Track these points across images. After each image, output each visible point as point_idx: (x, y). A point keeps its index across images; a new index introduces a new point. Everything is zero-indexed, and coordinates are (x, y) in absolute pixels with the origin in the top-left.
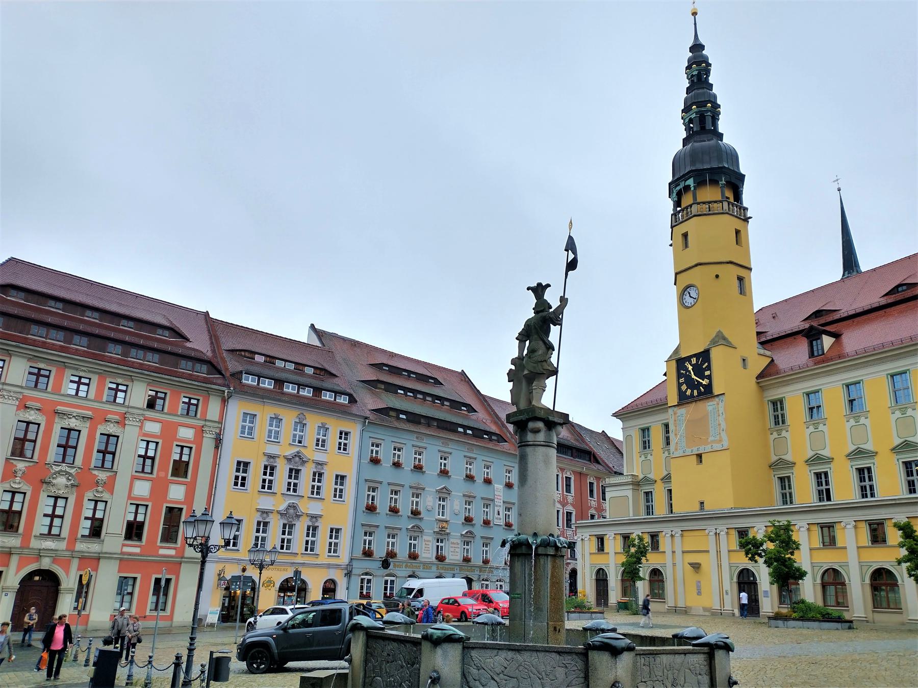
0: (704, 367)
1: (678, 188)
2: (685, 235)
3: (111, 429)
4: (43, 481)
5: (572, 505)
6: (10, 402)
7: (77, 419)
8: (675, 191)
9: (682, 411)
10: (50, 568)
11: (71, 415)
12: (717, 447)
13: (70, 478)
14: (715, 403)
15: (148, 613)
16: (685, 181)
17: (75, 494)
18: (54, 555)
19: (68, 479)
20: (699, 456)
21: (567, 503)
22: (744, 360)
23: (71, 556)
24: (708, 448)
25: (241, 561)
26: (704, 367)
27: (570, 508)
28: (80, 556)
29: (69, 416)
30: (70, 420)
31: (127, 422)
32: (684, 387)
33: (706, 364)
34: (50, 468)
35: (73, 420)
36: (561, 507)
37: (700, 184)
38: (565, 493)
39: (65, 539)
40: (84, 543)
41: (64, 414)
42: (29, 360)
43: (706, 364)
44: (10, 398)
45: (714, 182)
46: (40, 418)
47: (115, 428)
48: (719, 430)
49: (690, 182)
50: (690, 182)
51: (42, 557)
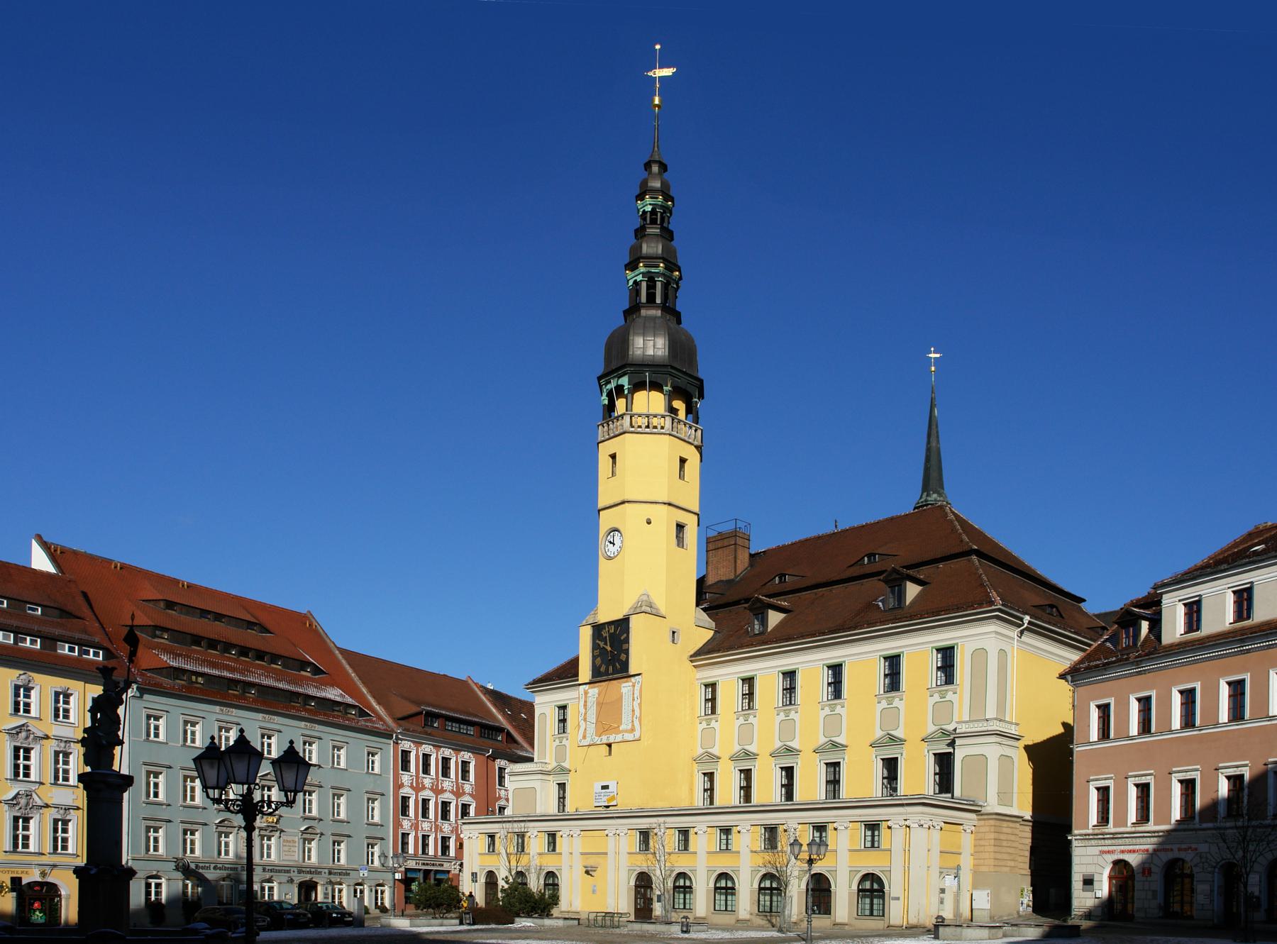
0: (622, 638)
1: (609, 387)
2: (613, 457)
5: (471, 795)
8: (605, 390)
9: (594, 691)
12: (629, 737)
14: (630, 684)
16: (619, 378)
20: (609, 745)
21: (464, 793)
22: (674, 633)
24: (619, 738)
26: (622, 638)
27: (466, 799)
32: (598, 661)
33: (625, 635)
36: (454, 797)
37: (638, 386)
38: (460, 781)
43: (625, 635)
45: (656, 386)
48: (633, 717)
49: (624, 381)
50: (624, 381)
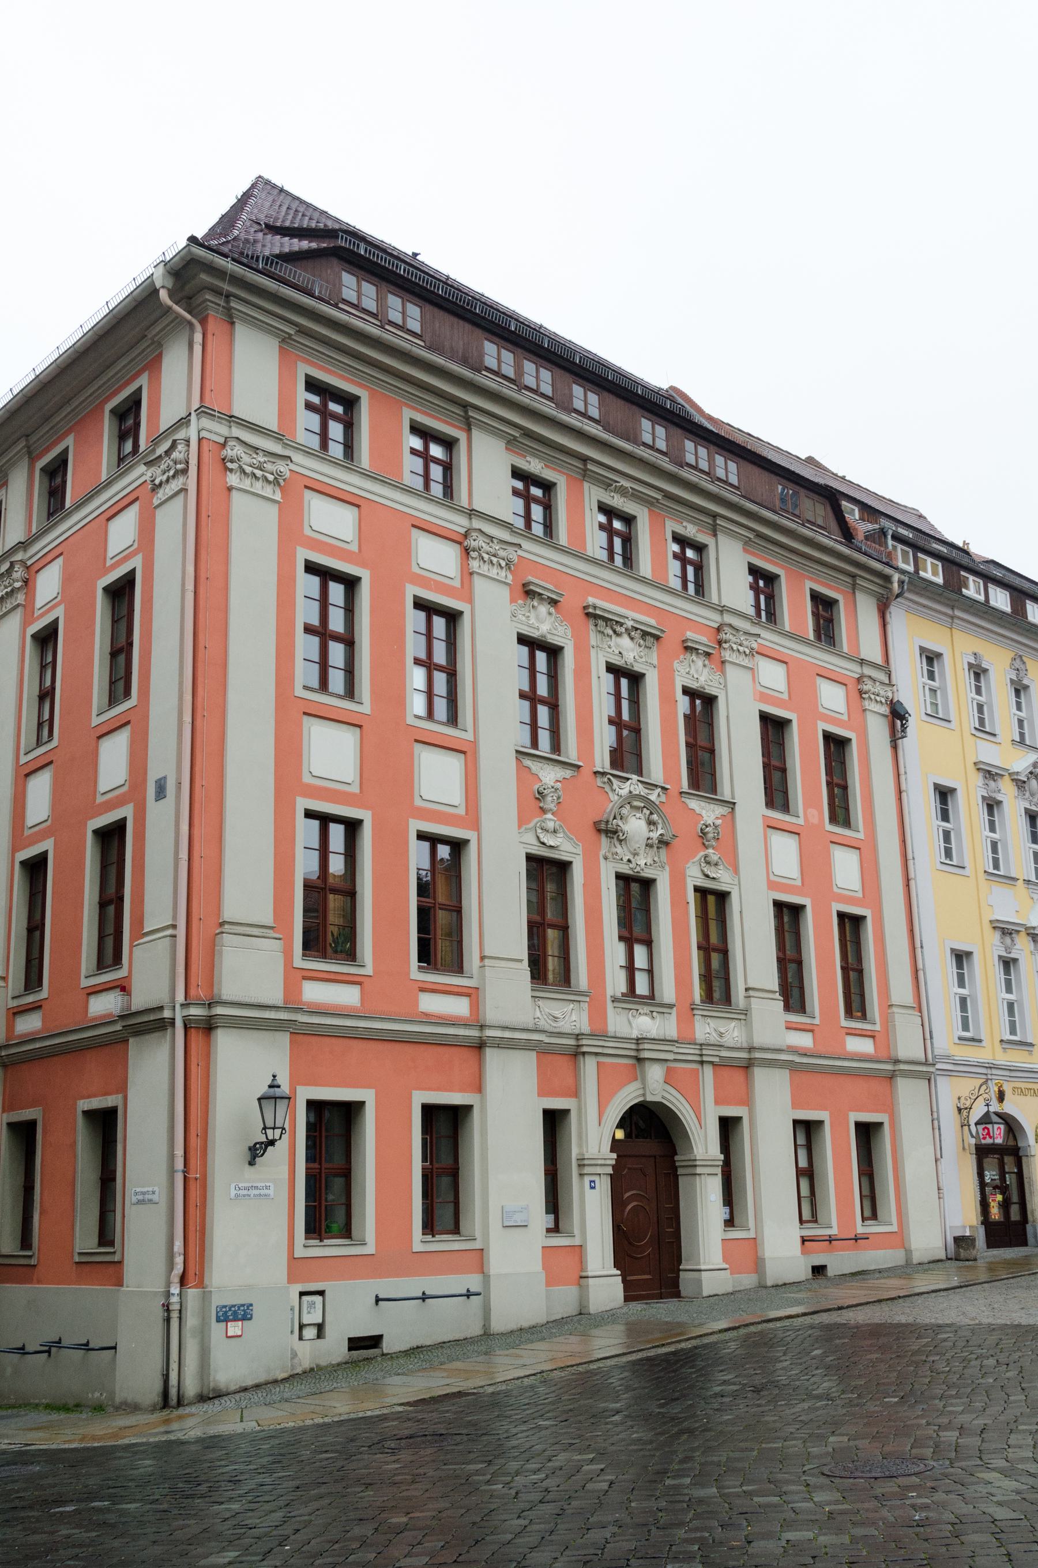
3: (701, 675)
4: (603, 826)
6: (494, 572)
7: (632, 639)
10: (663, 1097)
11: (621, 624)
13: (655, 817)
15: (860, 1229)
17: (667, 868)
18: (670, 1056)
19: (651, 823)
23: (698, 1058)
25: (994, 1072)
28: (716, 1059)
29: (618, 629)
30: (619, 640)
31: (727, 655)
34: (607, 788)
35: (625, 641)
39: (671, 1006)
40: (709, 1020)
41: (606, 620)
42: (511, 443)
44: (495, 560)
46: (561, 630)
47: (706, 670)
51: (647, 1064)
